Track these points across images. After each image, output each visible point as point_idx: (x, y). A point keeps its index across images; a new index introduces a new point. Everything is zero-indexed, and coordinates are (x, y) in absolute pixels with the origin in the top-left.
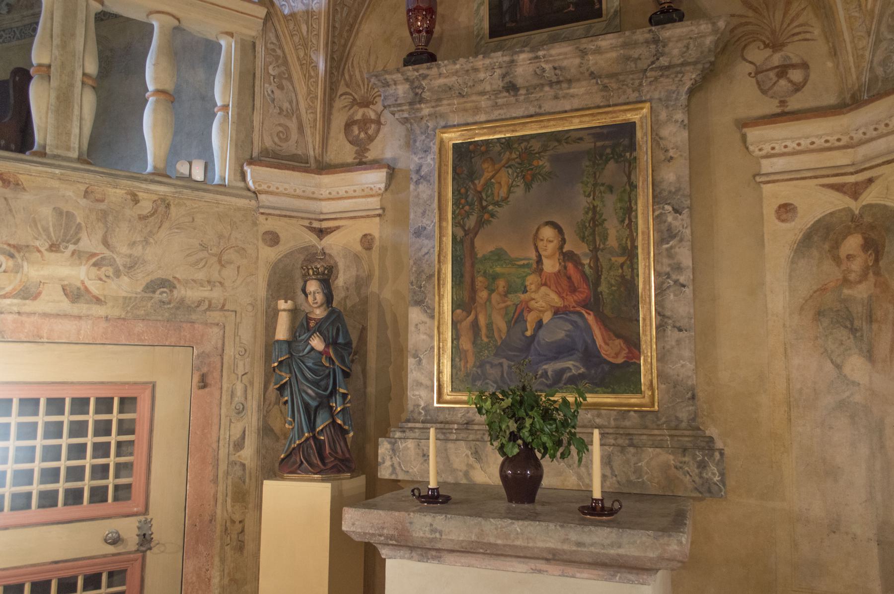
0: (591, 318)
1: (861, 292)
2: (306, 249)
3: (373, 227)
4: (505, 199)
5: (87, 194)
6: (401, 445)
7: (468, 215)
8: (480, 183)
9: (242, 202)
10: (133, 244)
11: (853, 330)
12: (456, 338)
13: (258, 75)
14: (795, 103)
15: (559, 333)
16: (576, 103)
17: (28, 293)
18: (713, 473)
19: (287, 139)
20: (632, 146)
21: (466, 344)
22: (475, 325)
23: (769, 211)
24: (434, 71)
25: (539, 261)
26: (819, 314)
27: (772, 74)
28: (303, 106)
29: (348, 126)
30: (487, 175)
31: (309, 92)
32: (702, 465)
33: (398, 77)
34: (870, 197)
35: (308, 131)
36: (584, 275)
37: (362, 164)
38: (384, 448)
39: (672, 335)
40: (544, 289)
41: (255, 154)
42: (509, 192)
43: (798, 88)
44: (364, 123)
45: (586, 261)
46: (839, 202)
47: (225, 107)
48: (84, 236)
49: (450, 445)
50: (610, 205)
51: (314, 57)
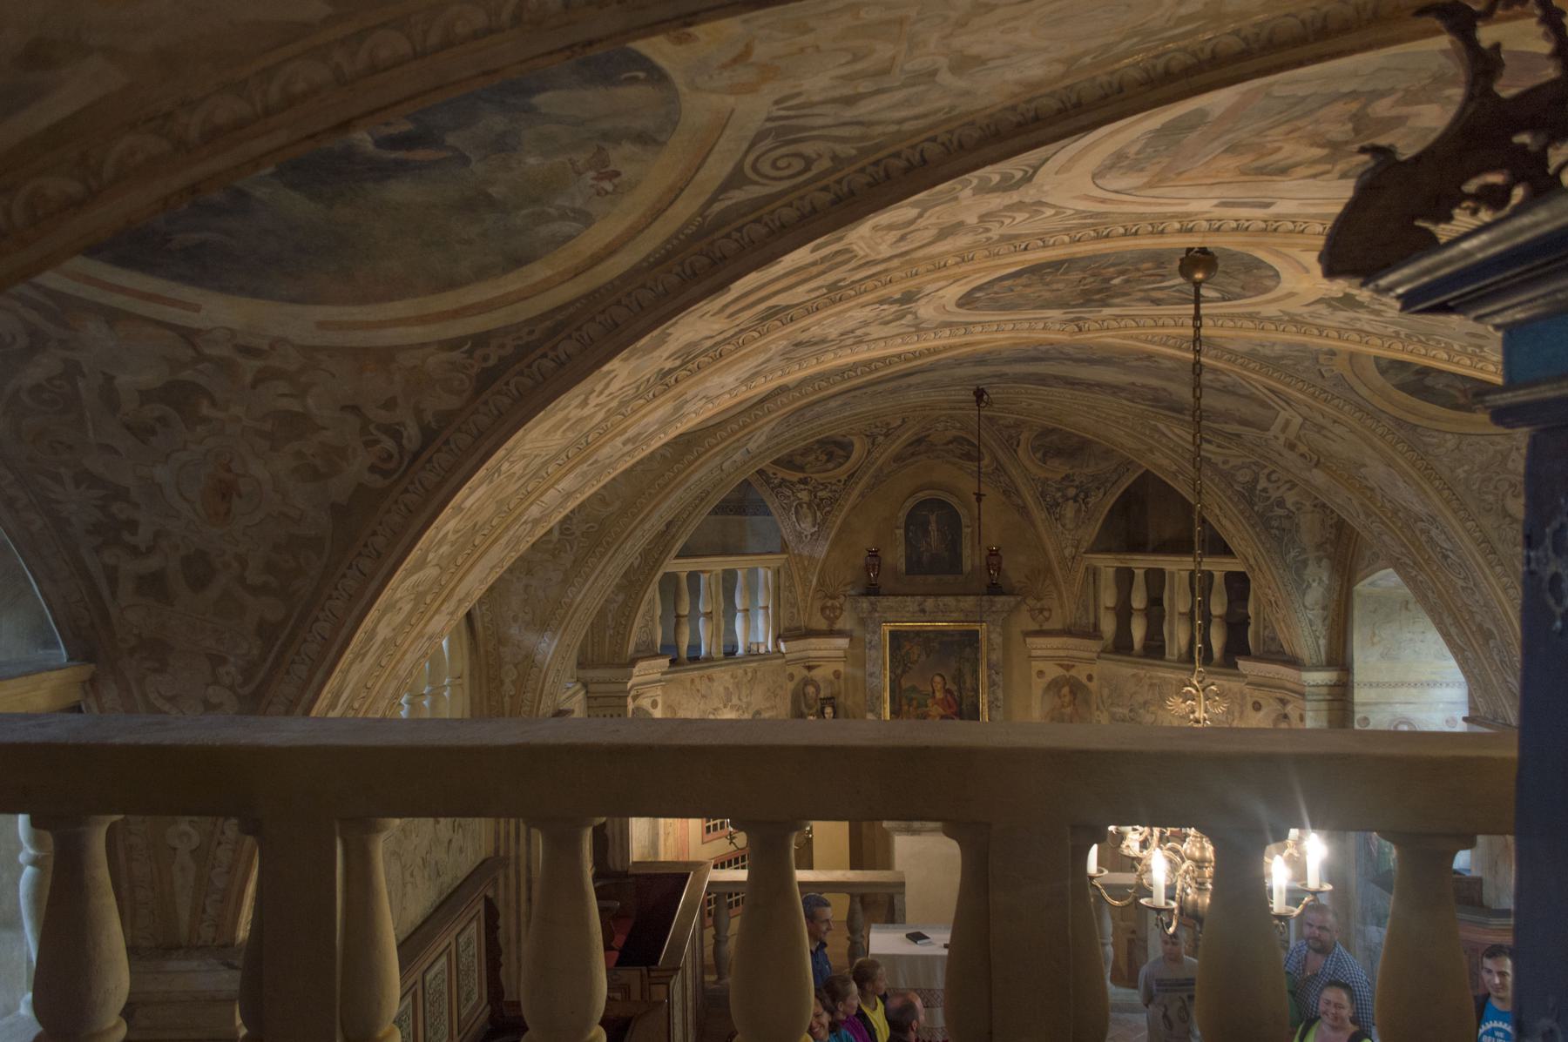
1: (1068, 710)
3: (841, 667)
5: (732, 676)
9: (779, 661)
13: (782, 588)
14: (1046, 627)
20: (977, 641)
23: (1034, 673)
25: (934, 692)
29: (823, 609)
31: (804, 593)
34: (1073, 672)
35: (801, 612)
36: (955, 699)
37: (831, 633)
42: (919, 657)
43: (1047, 619)
44: (833, 608)
45: (956, 694)
46: (1061, 672)
51: (810, 577)
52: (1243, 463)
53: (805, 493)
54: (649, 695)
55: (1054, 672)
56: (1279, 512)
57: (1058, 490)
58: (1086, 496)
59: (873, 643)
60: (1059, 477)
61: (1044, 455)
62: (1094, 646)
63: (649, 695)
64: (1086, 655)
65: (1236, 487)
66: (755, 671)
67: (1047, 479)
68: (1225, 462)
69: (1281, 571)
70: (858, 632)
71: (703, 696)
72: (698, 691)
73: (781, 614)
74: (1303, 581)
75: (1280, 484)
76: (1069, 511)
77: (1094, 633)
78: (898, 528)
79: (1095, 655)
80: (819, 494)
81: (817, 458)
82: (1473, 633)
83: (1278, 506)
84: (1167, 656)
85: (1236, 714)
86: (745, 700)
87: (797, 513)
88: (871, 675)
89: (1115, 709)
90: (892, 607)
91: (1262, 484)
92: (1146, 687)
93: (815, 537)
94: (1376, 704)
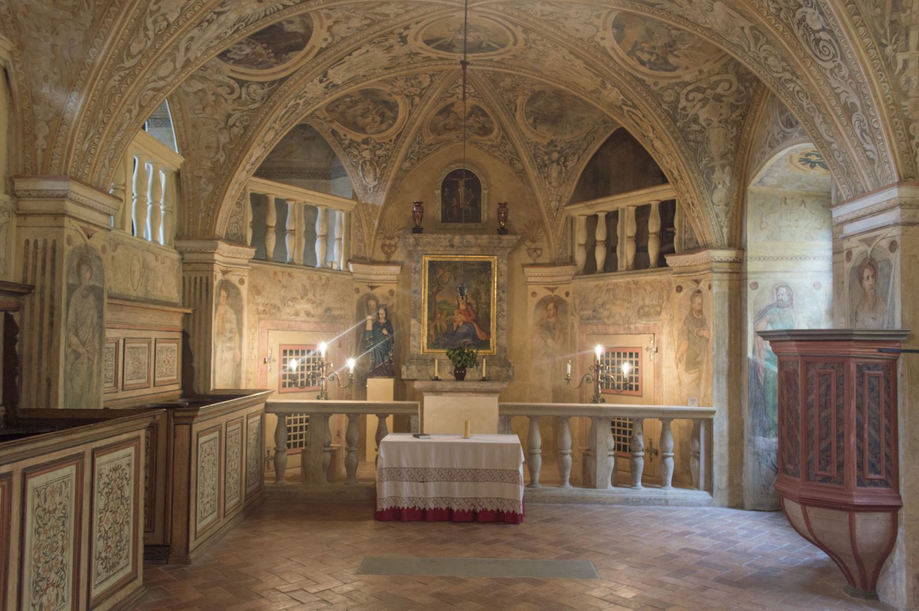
0: (475, 325)
1: (552, 320)
2: (367, 294)
3: (394, 287)
4: (447, 283)
5: (309, 278)
6: (410, 367)
7: (433, 287)
8: (438, 276)
9: (349, 277)
10: (321, 295)
11: (550, 331)
12: (429, 330)
13: (352, 226)
14: (539, 261)
15: (464, 329)
16: (473, 253)
17: (297, 314)
18: (510, 373)
19: (360, 251)
20: (490, 269)
21: (432, 333)
22: (435, 326)
23: (529, 294)
24: (425, 237)
25: (459, 305)
26: (542, 326)
27: (532, 251)
28: (366, 237)
29: (383, 246)
30: (440, 273)
31: (369, 233)
32: (508, 371)
33: (411, 236)
34: (556, 293)
35: (367, 248)
37: (388, 263)
38: (404, 369)
39: (500, 331)
40: (460, 315)
41: (351, 258)
43: (539, 256)
44: (390, 246)
45: (474, 306)
47: (340, 239)
48: (309, 293)
49: (429, 367)
50: (482, 288)
52: (669, 84)
53: (367, 152)
54: (238, 273)
55: (543, 293)
56: (695, 127)
57: (546, 153)
58: (566, 161)
59: (417, 269)
60: (545, 142)
61: (535, 121)
62: (569, 270)
63: (238, 273)
64: (565, 278)
65: (665, 106)
66: (328, 279)
67: (537, 143)
68: (656, 84)
69: (696, 175)
70: (407, 263)
71: (284, 286)
72: (280, 281)
73: (351, 245)
74: (712, 183)
75: (695, 102)
76: (554, 172)
77: (572, 261)
78: (437, 189)
79: (570, 277)
80: (378, 152)
81: (373, 120)
82: (838, 117)
83: (693, 122)
84: (619, 269)
85: (665, 298)
86: (319, 298)
87: (363, 169)
88: (415, 292)
89: (582, 313)
90: (430, 243)
91: (683, 103)
92: (604, 292)
93: (376, 189)
94: (764, 272)
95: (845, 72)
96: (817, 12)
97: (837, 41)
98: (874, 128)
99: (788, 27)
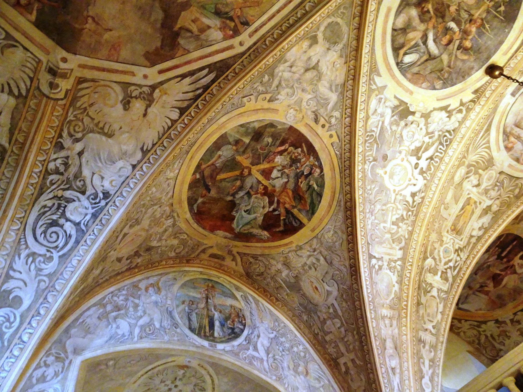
95: (50, 267)
96: (91, 211)
97: (77, 242)
98: (20, 338)
99: (41, 188)
